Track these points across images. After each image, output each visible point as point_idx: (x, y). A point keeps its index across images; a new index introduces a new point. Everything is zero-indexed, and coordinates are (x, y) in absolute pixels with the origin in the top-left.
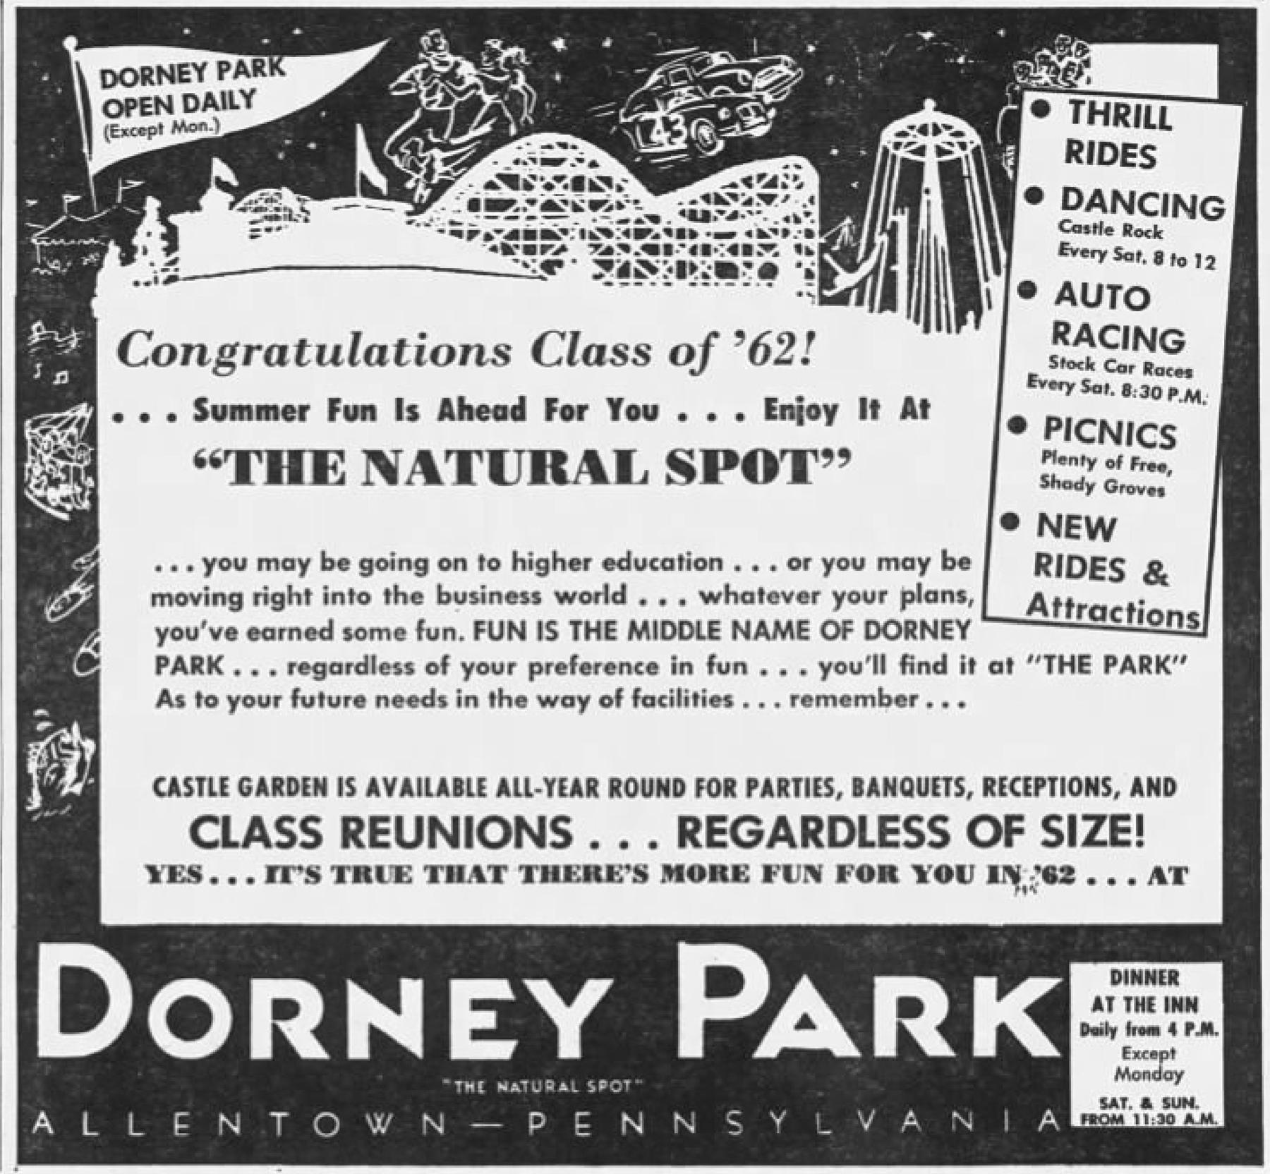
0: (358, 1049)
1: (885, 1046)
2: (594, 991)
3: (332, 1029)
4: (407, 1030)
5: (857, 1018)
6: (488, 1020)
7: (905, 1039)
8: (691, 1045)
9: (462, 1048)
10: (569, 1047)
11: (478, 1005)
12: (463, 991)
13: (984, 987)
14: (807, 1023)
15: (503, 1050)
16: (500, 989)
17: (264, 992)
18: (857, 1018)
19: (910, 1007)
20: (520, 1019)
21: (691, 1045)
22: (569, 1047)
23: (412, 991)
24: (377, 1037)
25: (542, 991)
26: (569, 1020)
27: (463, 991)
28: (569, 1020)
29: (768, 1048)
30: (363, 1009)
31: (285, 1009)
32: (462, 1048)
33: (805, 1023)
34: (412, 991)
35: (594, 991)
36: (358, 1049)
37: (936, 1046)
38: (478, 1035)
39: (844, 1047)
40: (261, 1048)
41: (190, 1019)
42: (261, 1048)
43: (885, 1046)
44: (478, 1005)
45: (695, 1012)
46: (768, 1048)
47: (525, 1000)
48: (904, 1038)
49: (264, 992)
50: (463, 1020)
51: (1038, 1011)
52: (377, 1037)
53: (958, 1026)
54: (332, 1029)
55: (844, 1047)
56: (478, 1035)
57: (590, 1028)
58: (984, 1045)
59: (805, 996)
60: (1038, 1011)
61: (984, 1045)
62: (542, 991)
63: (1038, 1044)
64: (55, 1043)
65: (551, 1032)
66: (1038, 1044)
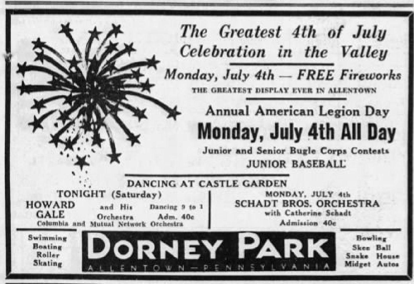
0: (163, 256)
1: (287, 255)
2: (219, 243)
3: (157, 252)
4: (174, 252)
5: (281, 250)
6: (193, 250)
7: (292, 254)
8: (241, 255)
9: (187, 256)
10: (213, 256)
11: (191, 246)
12: (187, 243)
13: (310, 241)
14: (269, 250)
15: (197, 257)
16: (196, 243)
17: (141, 243)
18: (281, 250)
19: (293, 246)
20: (200, 249)
21: (241, 255)
22: (213, 256)
23: (175, 243)
24: (167, 254)
25: (206, 243)
26: (213, 249)
27: (187, 243)
28: (213, 249)
29: (260, 256)
30: (164, 247)
31: (146, 247)
32: (187, 256)
33: (268, 250)
34: (175, 243)
35: (219, 243)
36: (163, 256)
37: (299, 255)
38: (191, 253)
39: (277, 255)
40: (140, 256)
41: (123, 250)
42: (140, 256)
43: (287, 255)
44: (191, 246)
45: (242, 247)
46: (260, 256)
47: (202, 245)
48: (292, 254)
49: (141, 243)
50: (188, 250)
51: (323, 247)
52: (167, 254)
53: (304, 251)
54: (157, 252)
55: (277, 255)
56: (191, 253)
57: (218, 252)
58: (311, 255)
59: (268, 244)
60: (323, 247)
61: (311, 255)
62: (206, 243)
63: (324, 255)
64: (92, 255)
65: (208, 253)
66: (324, 255)
